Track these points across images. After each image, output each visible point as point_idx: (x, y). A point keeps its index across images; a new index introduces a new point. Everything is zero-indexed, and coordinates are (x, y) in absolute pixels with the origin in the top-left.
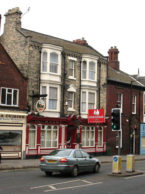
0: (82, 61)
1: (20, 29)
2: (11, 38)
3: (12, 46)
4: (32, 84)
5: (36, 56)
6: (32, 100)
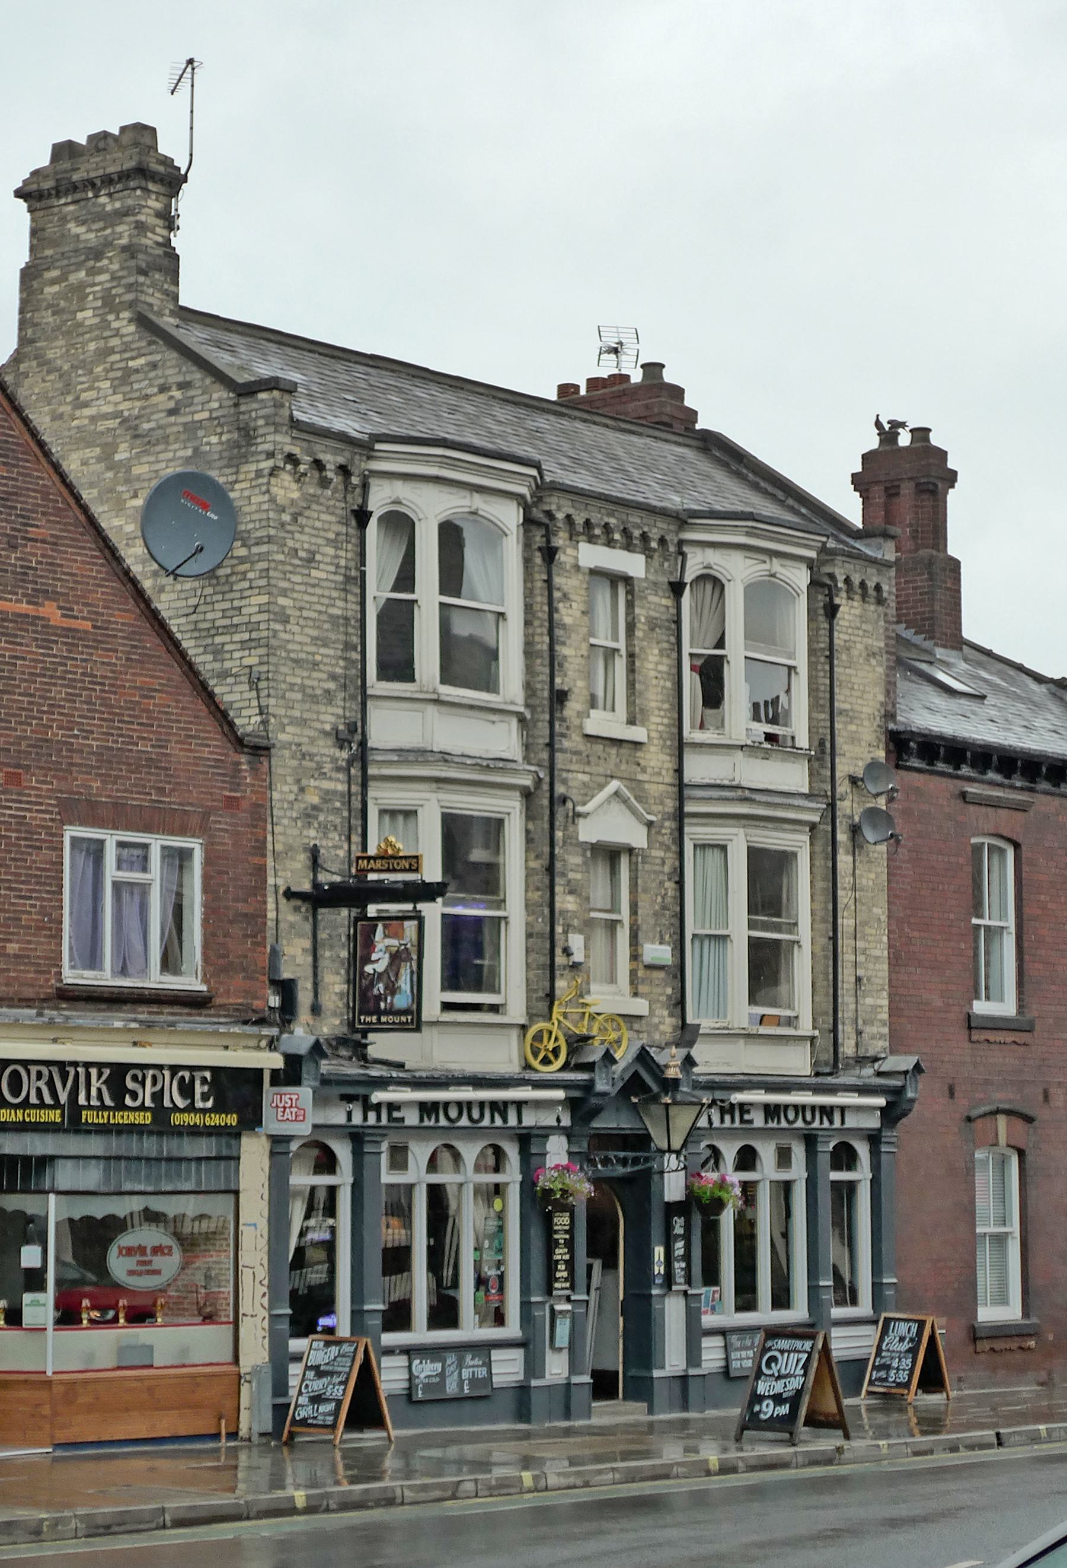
0: (688, 578)
1: (173, 313)
2: (92, 394)
3: (109, 468)
4: (302, 790)
5: (331, 551)
6: (308, 927)
